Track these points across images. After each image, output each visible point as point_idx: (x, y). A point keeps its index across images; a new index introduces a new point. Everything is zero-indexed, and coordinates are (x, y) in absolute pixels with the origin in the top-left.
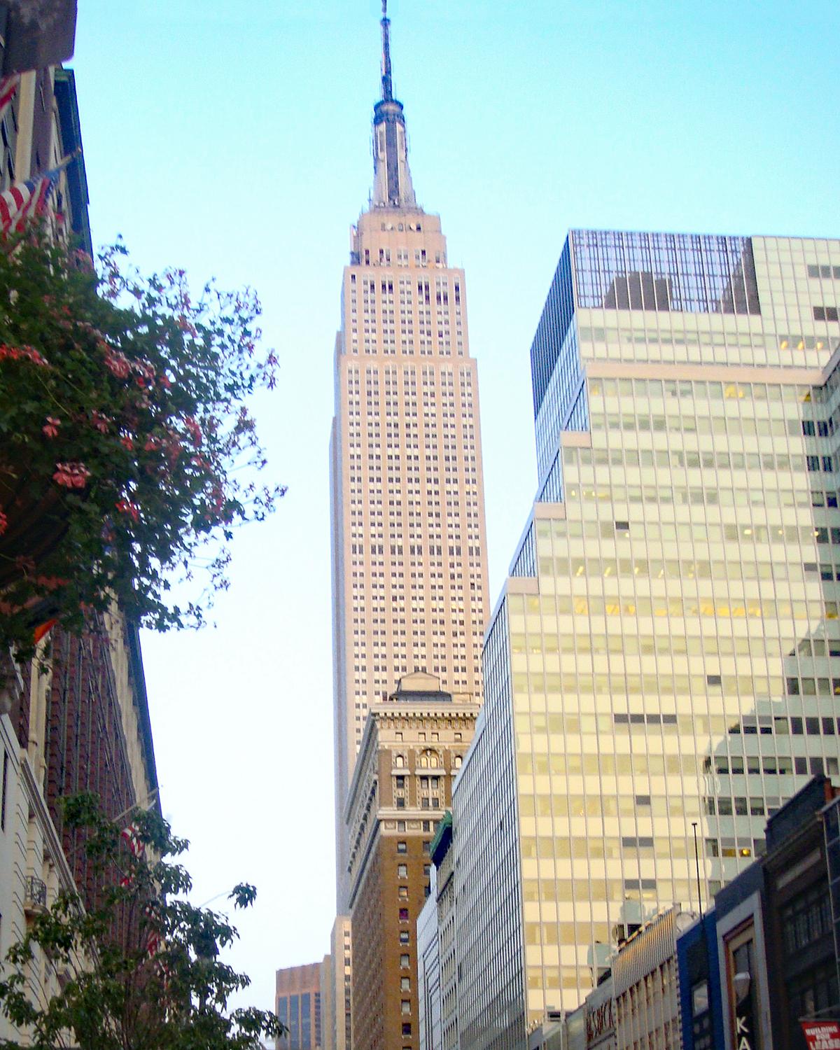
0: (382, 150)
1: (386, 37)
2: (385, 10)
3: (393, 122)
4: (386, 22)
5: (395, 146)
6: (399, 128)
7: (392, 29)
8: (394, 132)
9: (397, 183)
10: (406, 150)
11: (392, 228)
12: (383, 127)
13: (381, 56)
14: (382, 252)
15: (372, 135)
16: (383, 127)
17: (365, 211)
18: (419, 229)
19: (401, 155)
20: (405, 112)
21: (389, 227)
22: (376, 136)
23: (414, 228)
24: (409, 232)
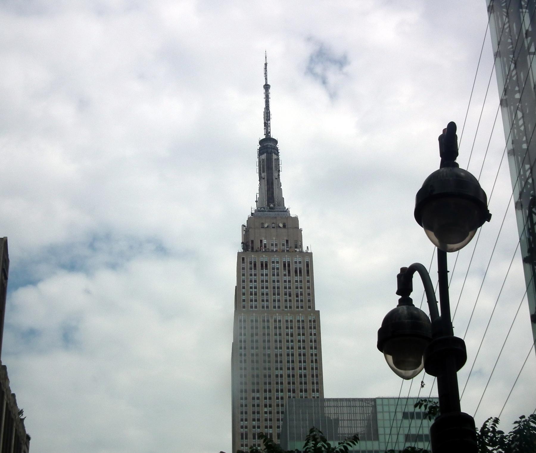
0: (263, 172)
2: (266, 79)
3: (271, 153)
4: (267, 87)
5: (272, 169)
6: (274, 157)
7: (271, 91)
8: (271, 159)
9: (273, 193)
10: (279, 171)
11: (268, 227)
12: (264, 156)
14: (261, 241)
15: (257, 160)
16: (264, 156)
17: (253, 212)
18: (284, 226)
19: (275, 175)
20: (279, 146)
21: (266, 226)
22: (260, 162)
23: (281, 225)
24: (279, 229)
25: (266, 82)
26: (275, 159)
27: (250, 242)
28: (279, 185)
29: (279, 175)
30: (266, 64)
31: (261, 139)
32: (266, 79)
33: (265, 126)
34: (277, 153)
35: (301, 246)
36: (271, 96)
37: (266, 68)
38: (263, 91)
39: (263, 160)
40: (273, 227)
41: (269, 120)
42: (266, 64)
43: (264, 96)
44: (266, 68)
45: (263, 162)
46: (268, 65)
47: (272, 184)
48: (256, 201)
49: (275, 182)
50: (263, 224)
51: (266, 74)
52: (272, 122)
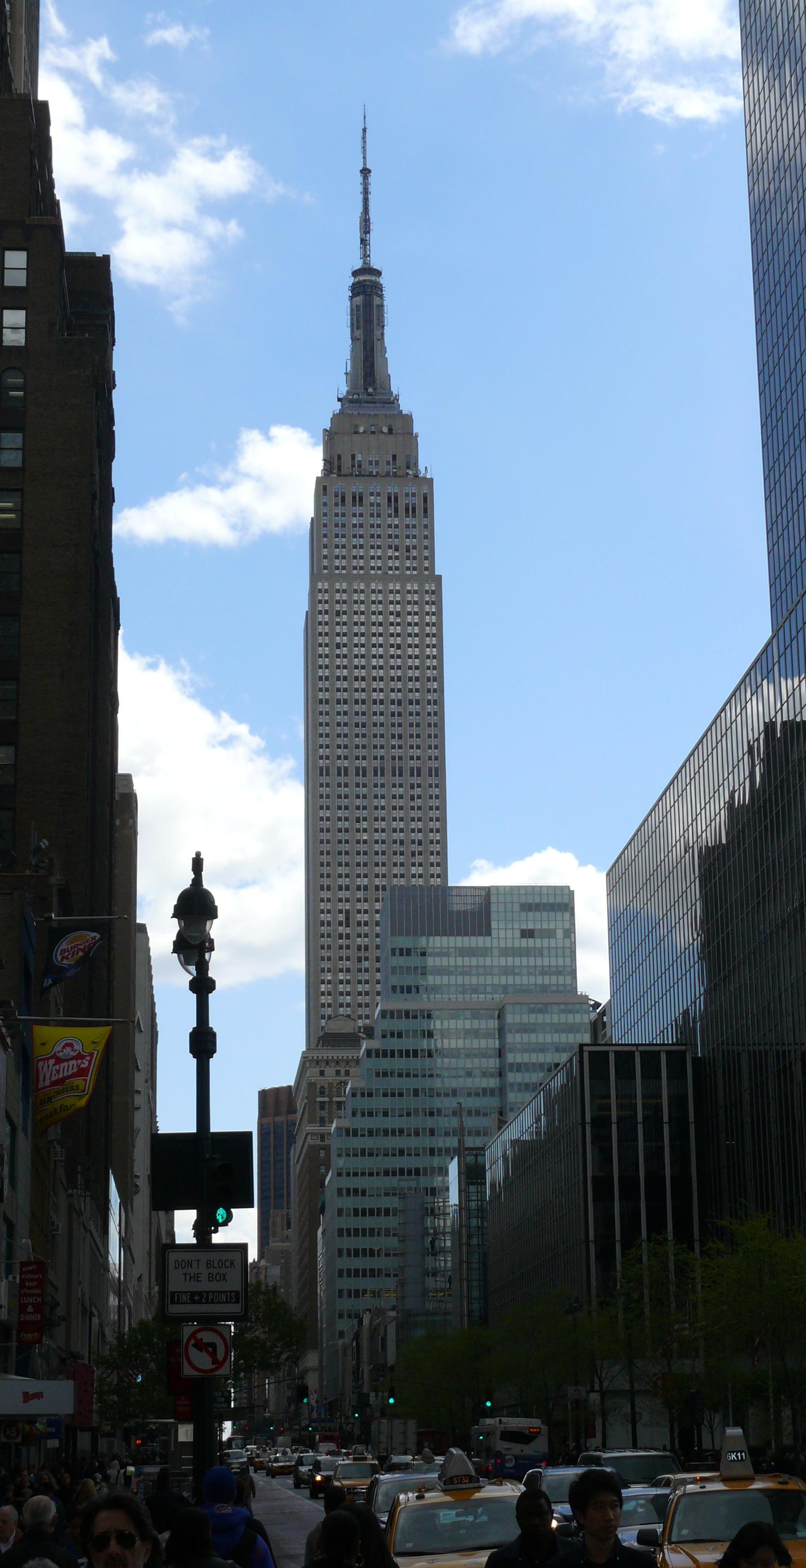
0: (358, 328)
1: (366, 192)
4: (365, 172)
5: (371, 321)
6: (376, 301)
7: (372, 179)
9: (372, 364)
10: (383, 326)
11: (364, 432)
12: (359, 300)
13: (360, 208)
14: (353, 457)
16: (359, 300)
17: (341, 396)
18: (390, 430)
19: (377, 333)
20: (382, 280)
21: (361, 430)
22: (352, 310)
23: (385, 430)
24: (382, 436)
25: (365, 164)
26: (378, 306)
27: (336, 458)
28: (384, 350)
29: (383, 334)
30: (364, 130)
31: (356, 268)
32: (364, 158)
33: (361, 243)
34: (381, 297)
35: (416, 464)
36: (372, 188)
37: (364, 138)
38: (359, 178)
39: (357, 306)
40: (373, 433)
41: (369, 232)
42: (364, 130)
43: (360, 188)
44: (364, 138)
45: (358, 310)
46: (367, 130)
47: (372, 349)
48: (346, 374)
49: (377, 345)
50: (356, 426)
51: (364, 148)
52: (373, 237)
